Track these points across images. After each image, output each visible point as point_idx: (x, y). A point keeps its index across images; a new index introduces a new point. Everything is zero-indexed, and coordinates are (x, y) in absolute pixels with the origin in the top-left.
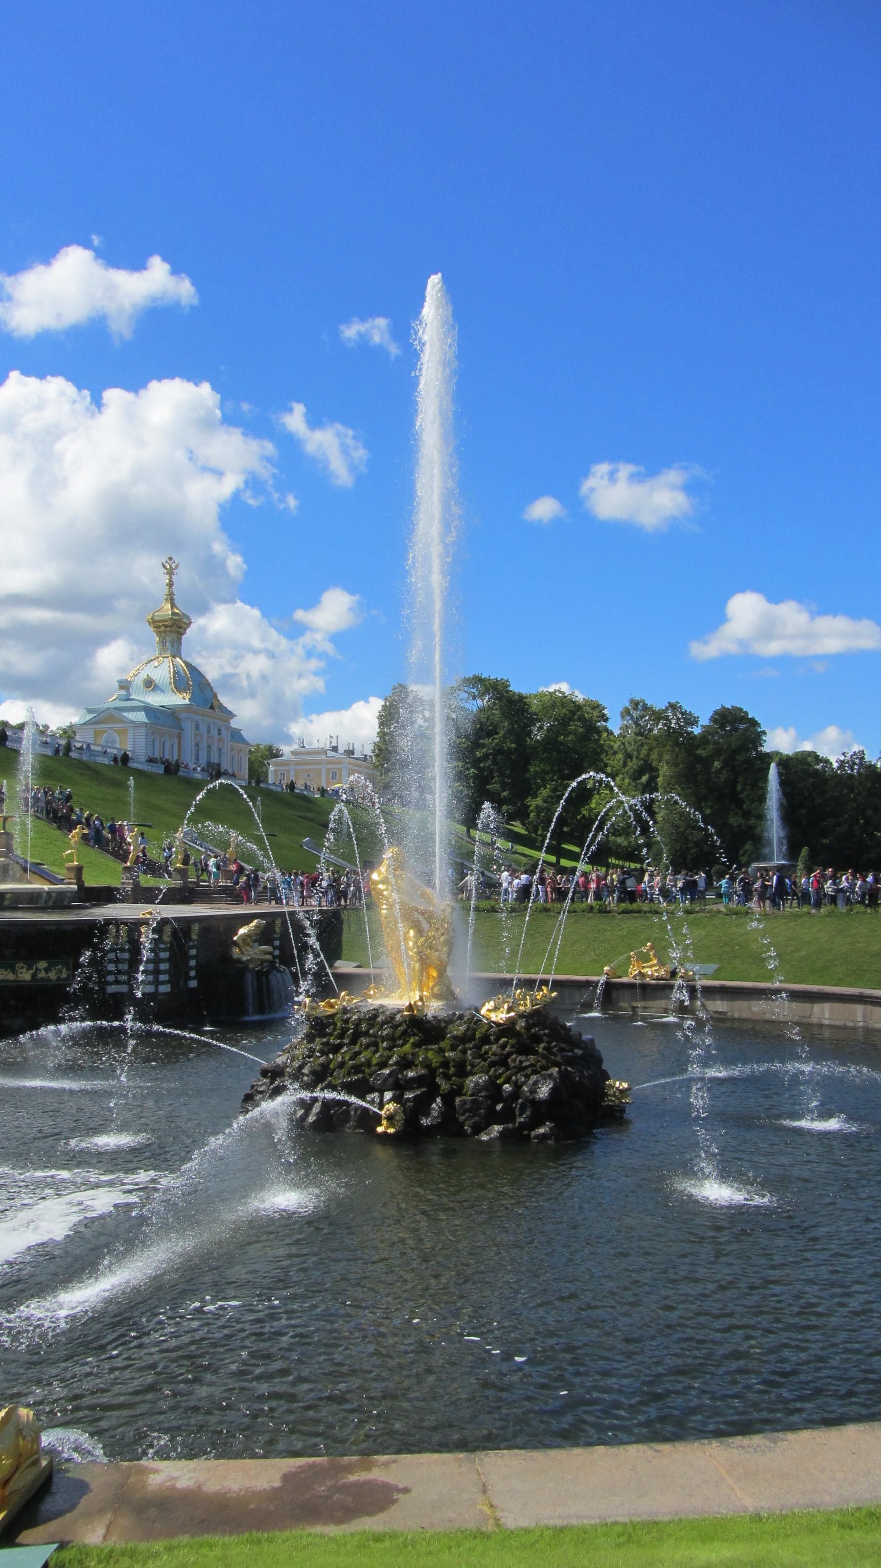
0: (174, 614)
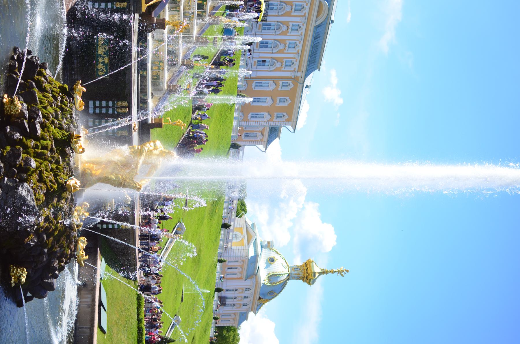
0: (315, 274)
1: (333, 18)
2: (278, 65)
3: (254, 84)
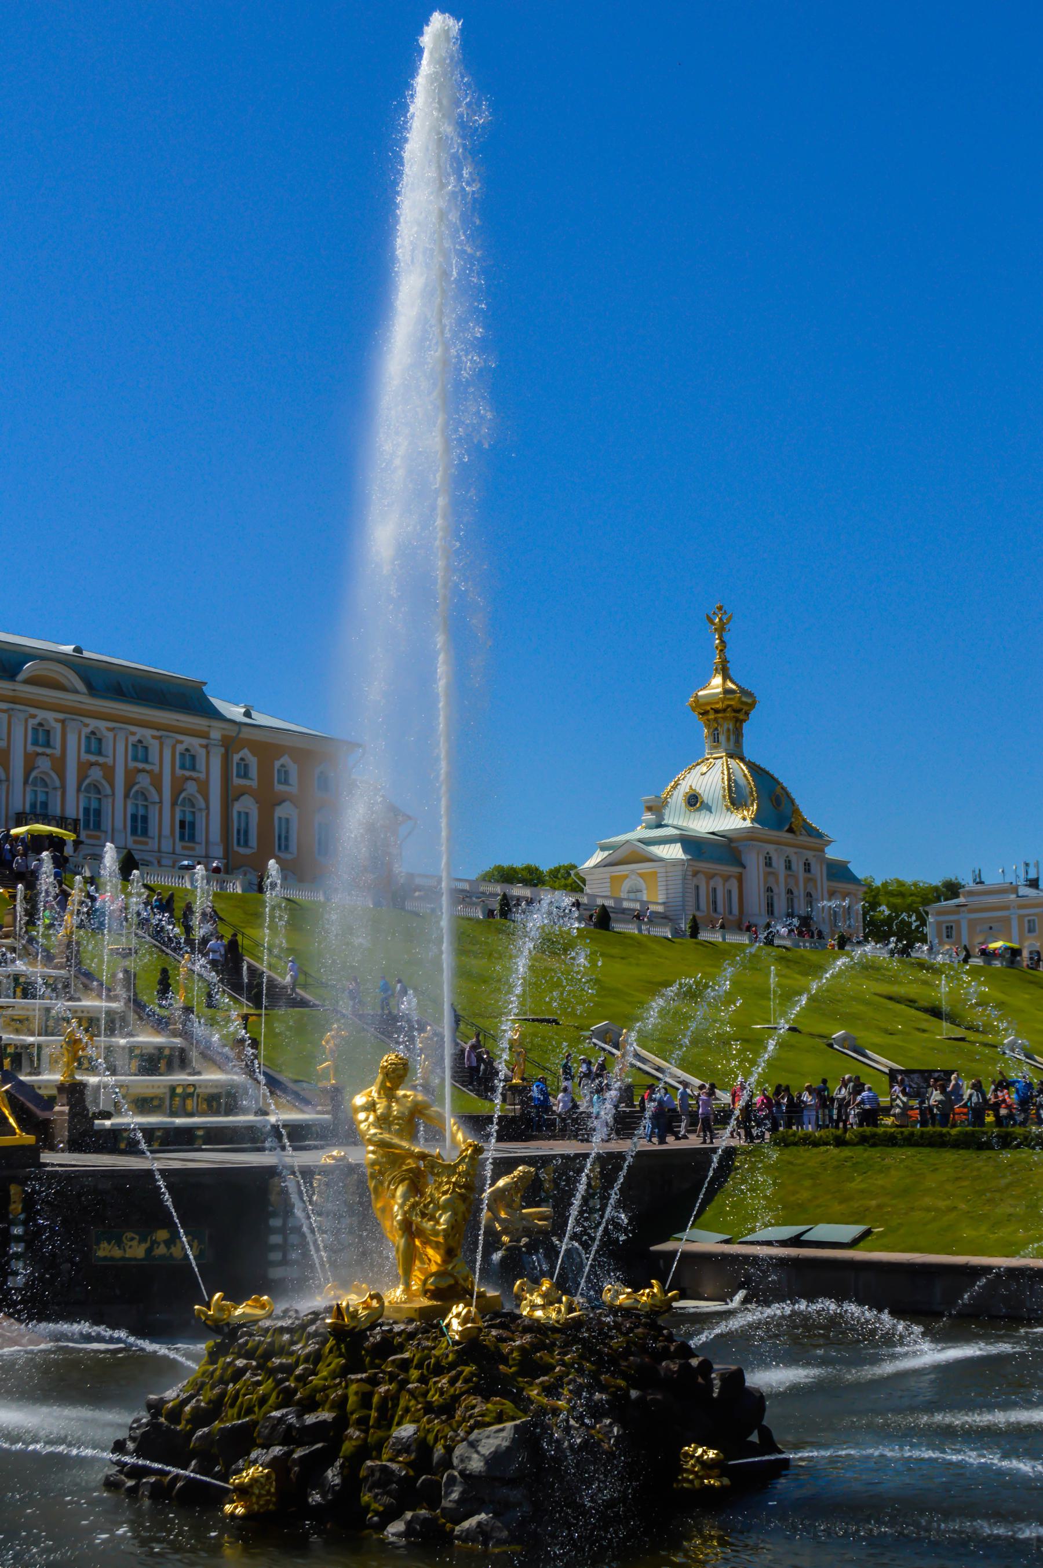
0: (727, 691)
1: (69, 649)
2: (191, 788)
3: (242, 850)
